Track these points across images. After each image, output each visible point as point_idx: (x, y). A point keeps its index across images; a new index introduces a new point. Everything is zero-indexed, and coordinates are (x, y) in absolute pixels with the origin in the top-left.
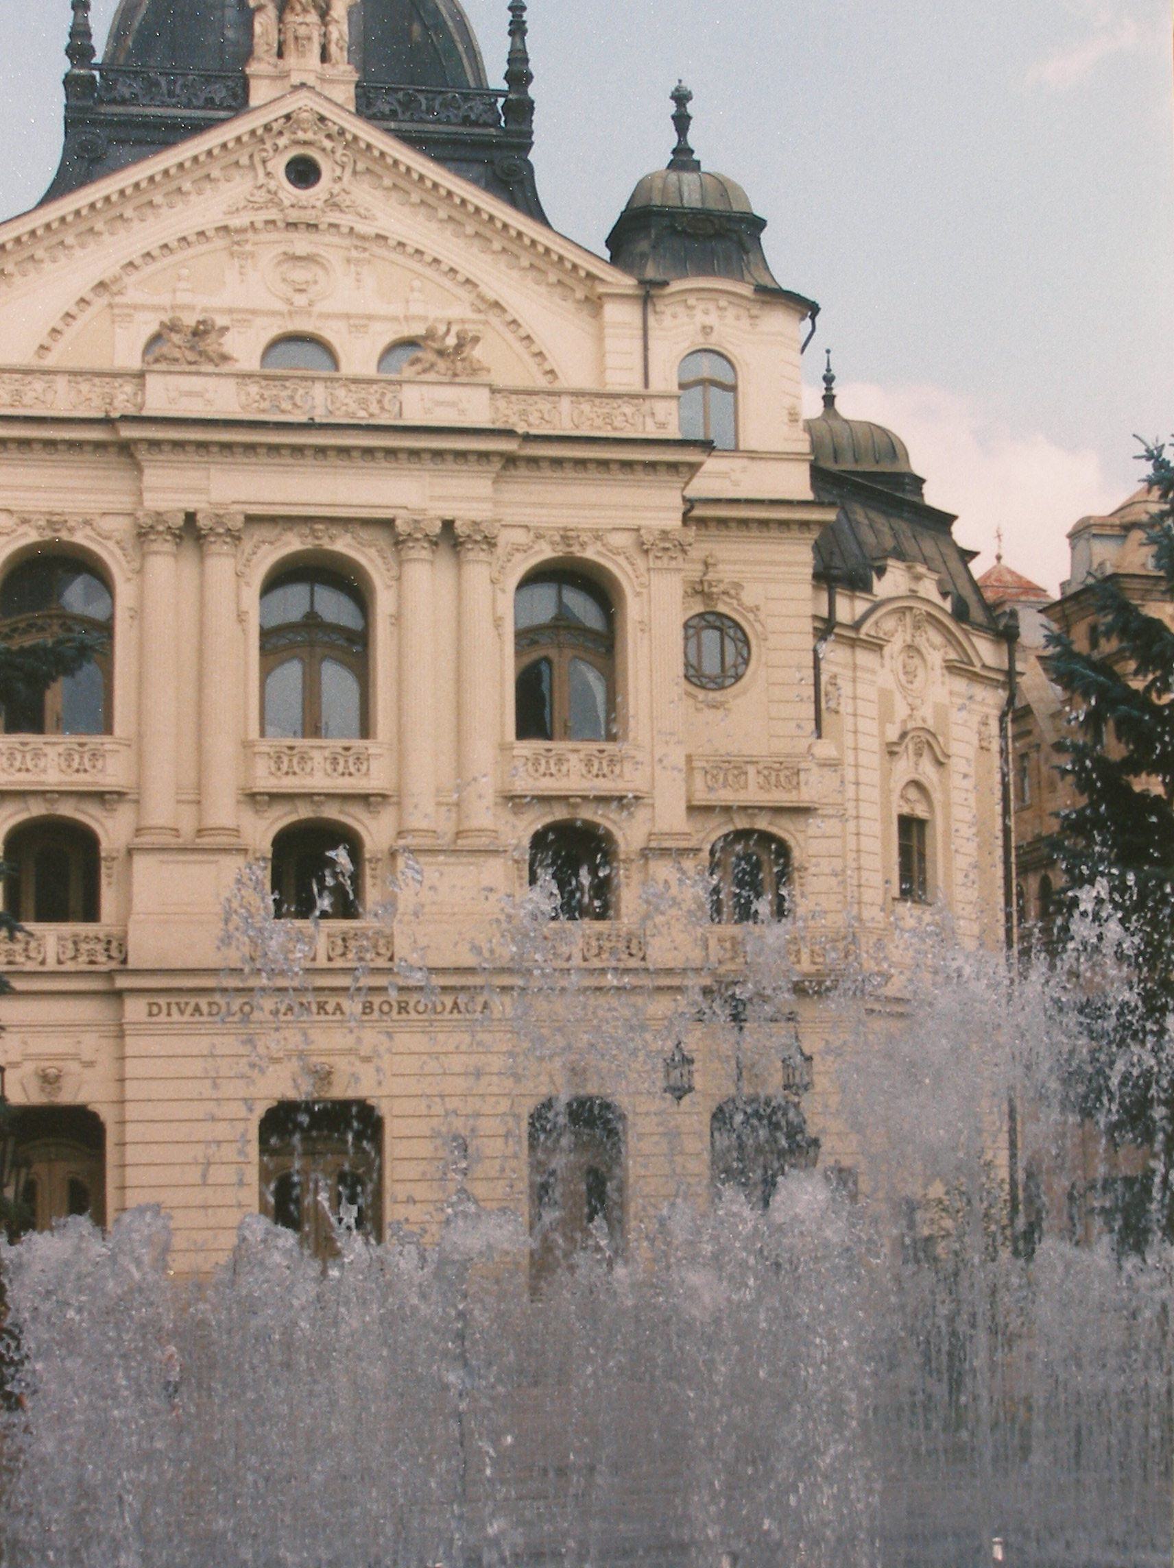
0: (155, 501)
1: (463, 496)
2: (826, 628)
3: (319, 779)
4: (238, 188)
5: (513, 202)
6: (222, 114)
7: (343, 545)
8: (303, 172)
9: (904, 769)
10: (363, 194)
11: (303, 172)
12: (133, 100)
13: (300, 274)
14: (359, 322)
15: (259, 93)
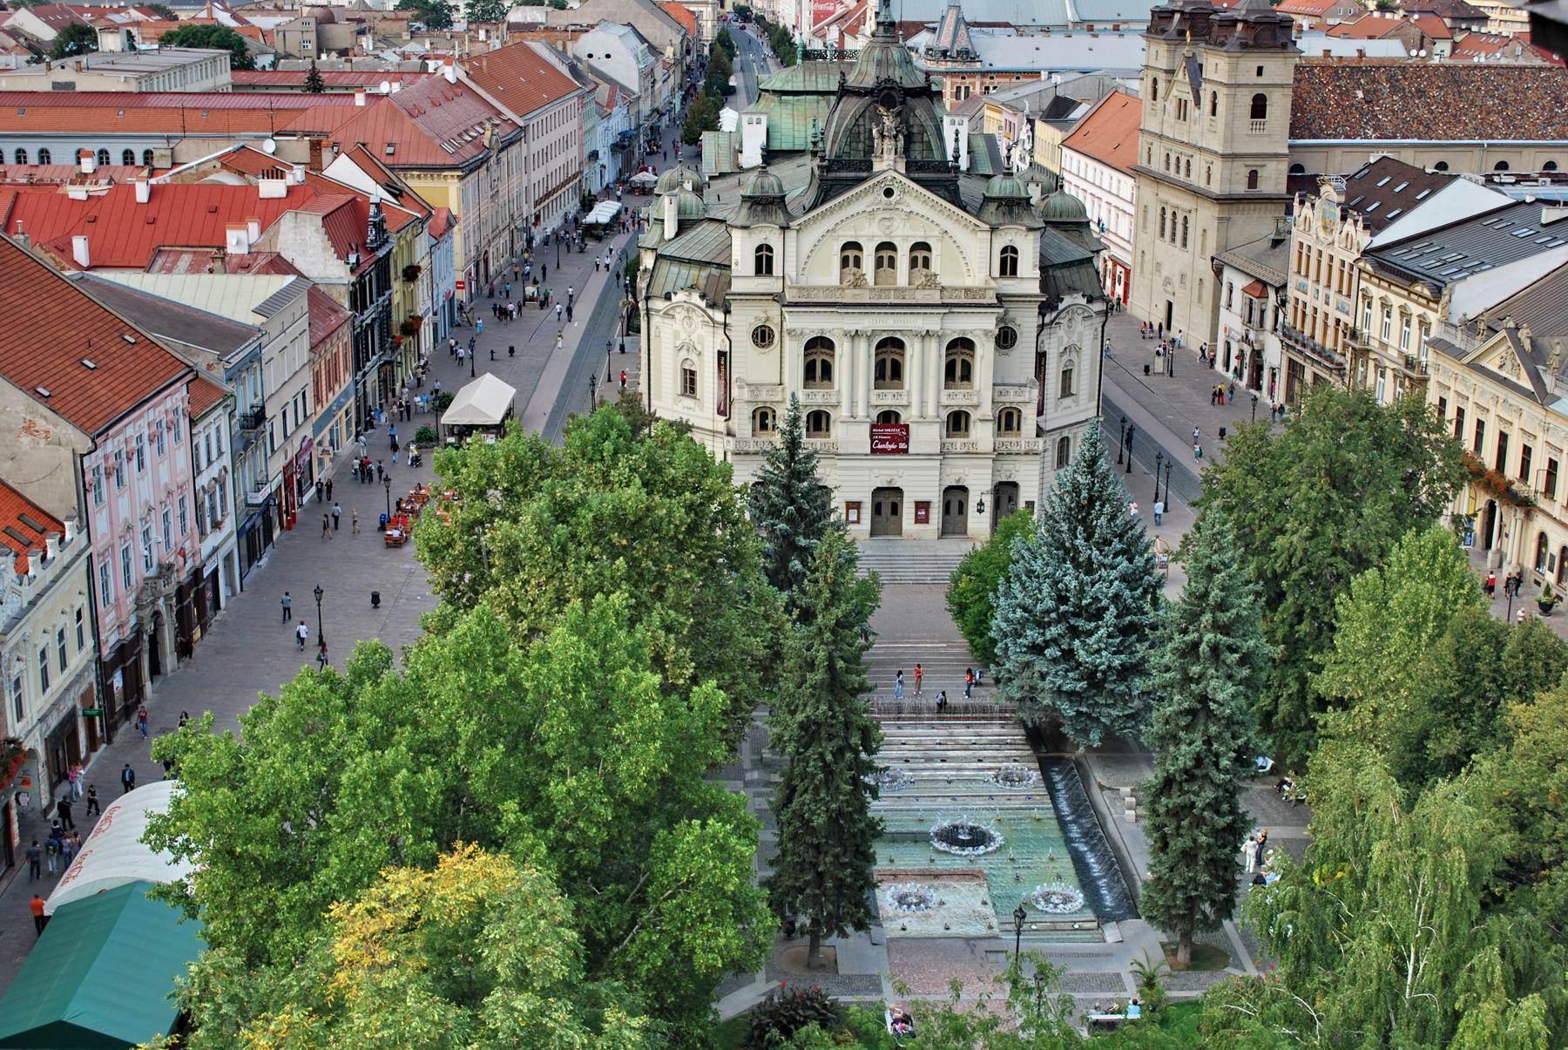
0: (847, 328)
1: (932, 323)
2: (1042, 327)
3: (890, 402)
4: (870, 198)
5: (953, 203)
6: (865, 174)
7: (898, 336)
8: (888, 193)
9: (1066, 358)
10: (907, 198)
11: (888, 193)
12: (839, 170)
13: (887, 223)
14: (906, 238)
15: (877, 167)
